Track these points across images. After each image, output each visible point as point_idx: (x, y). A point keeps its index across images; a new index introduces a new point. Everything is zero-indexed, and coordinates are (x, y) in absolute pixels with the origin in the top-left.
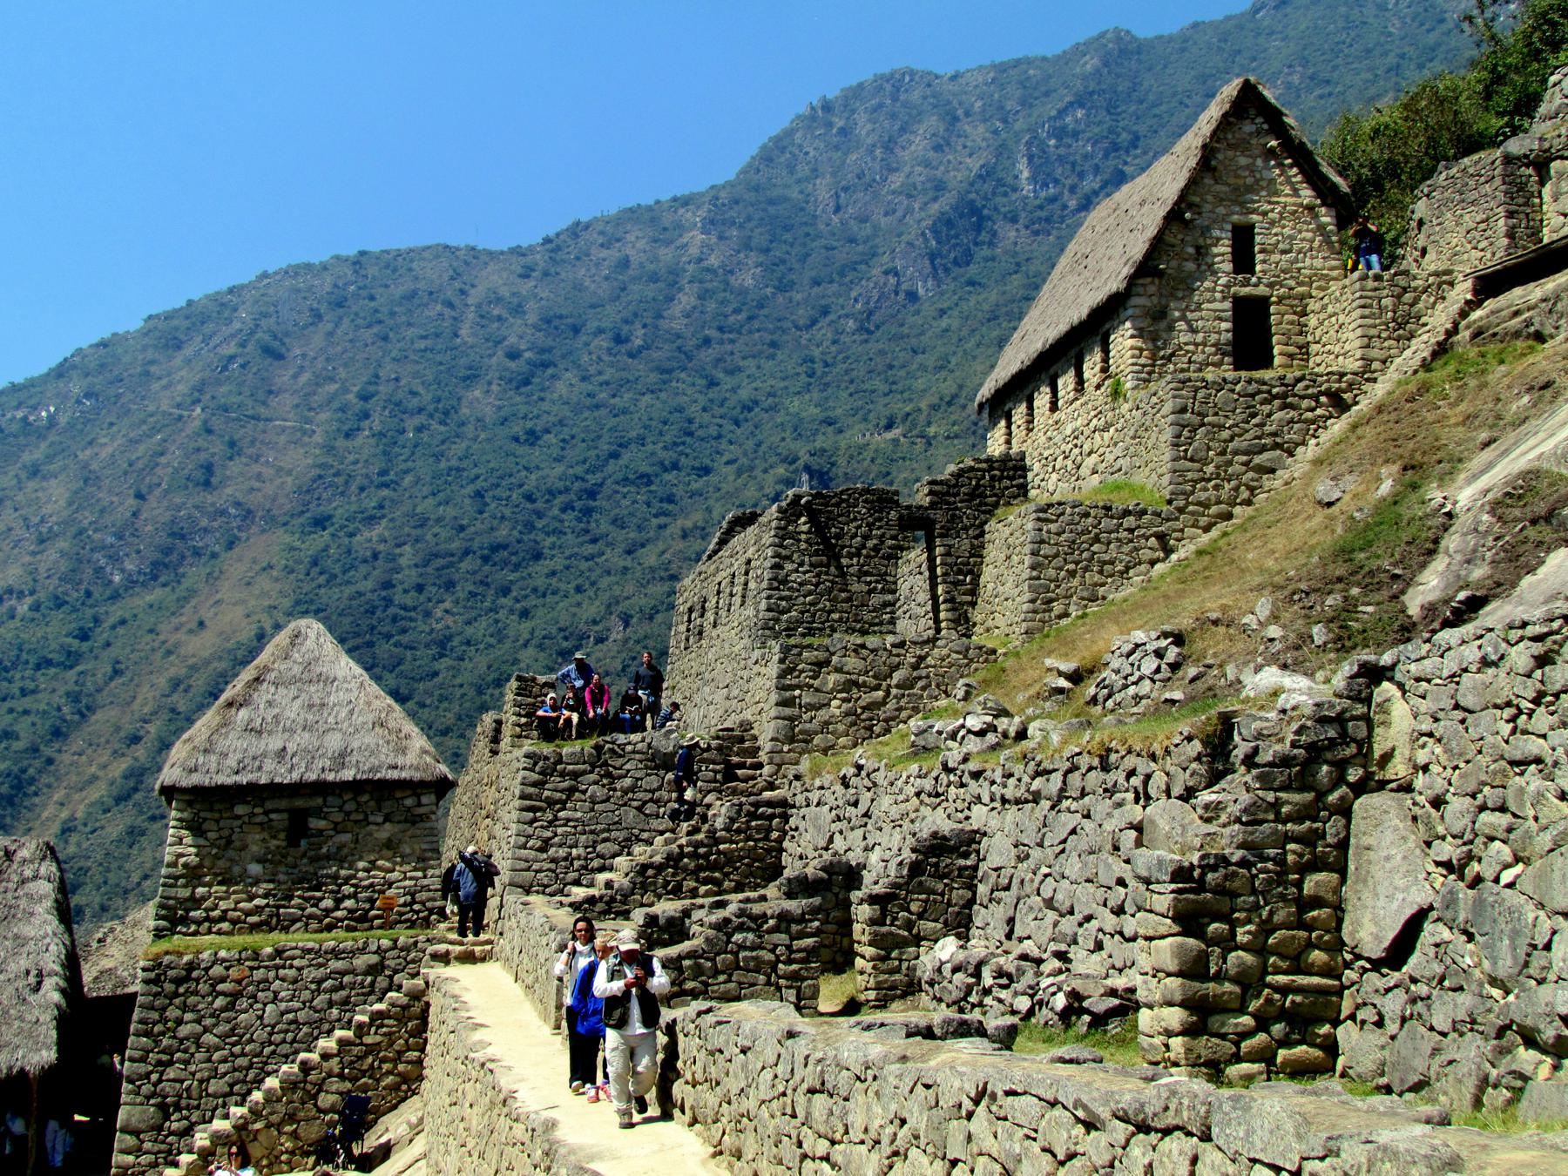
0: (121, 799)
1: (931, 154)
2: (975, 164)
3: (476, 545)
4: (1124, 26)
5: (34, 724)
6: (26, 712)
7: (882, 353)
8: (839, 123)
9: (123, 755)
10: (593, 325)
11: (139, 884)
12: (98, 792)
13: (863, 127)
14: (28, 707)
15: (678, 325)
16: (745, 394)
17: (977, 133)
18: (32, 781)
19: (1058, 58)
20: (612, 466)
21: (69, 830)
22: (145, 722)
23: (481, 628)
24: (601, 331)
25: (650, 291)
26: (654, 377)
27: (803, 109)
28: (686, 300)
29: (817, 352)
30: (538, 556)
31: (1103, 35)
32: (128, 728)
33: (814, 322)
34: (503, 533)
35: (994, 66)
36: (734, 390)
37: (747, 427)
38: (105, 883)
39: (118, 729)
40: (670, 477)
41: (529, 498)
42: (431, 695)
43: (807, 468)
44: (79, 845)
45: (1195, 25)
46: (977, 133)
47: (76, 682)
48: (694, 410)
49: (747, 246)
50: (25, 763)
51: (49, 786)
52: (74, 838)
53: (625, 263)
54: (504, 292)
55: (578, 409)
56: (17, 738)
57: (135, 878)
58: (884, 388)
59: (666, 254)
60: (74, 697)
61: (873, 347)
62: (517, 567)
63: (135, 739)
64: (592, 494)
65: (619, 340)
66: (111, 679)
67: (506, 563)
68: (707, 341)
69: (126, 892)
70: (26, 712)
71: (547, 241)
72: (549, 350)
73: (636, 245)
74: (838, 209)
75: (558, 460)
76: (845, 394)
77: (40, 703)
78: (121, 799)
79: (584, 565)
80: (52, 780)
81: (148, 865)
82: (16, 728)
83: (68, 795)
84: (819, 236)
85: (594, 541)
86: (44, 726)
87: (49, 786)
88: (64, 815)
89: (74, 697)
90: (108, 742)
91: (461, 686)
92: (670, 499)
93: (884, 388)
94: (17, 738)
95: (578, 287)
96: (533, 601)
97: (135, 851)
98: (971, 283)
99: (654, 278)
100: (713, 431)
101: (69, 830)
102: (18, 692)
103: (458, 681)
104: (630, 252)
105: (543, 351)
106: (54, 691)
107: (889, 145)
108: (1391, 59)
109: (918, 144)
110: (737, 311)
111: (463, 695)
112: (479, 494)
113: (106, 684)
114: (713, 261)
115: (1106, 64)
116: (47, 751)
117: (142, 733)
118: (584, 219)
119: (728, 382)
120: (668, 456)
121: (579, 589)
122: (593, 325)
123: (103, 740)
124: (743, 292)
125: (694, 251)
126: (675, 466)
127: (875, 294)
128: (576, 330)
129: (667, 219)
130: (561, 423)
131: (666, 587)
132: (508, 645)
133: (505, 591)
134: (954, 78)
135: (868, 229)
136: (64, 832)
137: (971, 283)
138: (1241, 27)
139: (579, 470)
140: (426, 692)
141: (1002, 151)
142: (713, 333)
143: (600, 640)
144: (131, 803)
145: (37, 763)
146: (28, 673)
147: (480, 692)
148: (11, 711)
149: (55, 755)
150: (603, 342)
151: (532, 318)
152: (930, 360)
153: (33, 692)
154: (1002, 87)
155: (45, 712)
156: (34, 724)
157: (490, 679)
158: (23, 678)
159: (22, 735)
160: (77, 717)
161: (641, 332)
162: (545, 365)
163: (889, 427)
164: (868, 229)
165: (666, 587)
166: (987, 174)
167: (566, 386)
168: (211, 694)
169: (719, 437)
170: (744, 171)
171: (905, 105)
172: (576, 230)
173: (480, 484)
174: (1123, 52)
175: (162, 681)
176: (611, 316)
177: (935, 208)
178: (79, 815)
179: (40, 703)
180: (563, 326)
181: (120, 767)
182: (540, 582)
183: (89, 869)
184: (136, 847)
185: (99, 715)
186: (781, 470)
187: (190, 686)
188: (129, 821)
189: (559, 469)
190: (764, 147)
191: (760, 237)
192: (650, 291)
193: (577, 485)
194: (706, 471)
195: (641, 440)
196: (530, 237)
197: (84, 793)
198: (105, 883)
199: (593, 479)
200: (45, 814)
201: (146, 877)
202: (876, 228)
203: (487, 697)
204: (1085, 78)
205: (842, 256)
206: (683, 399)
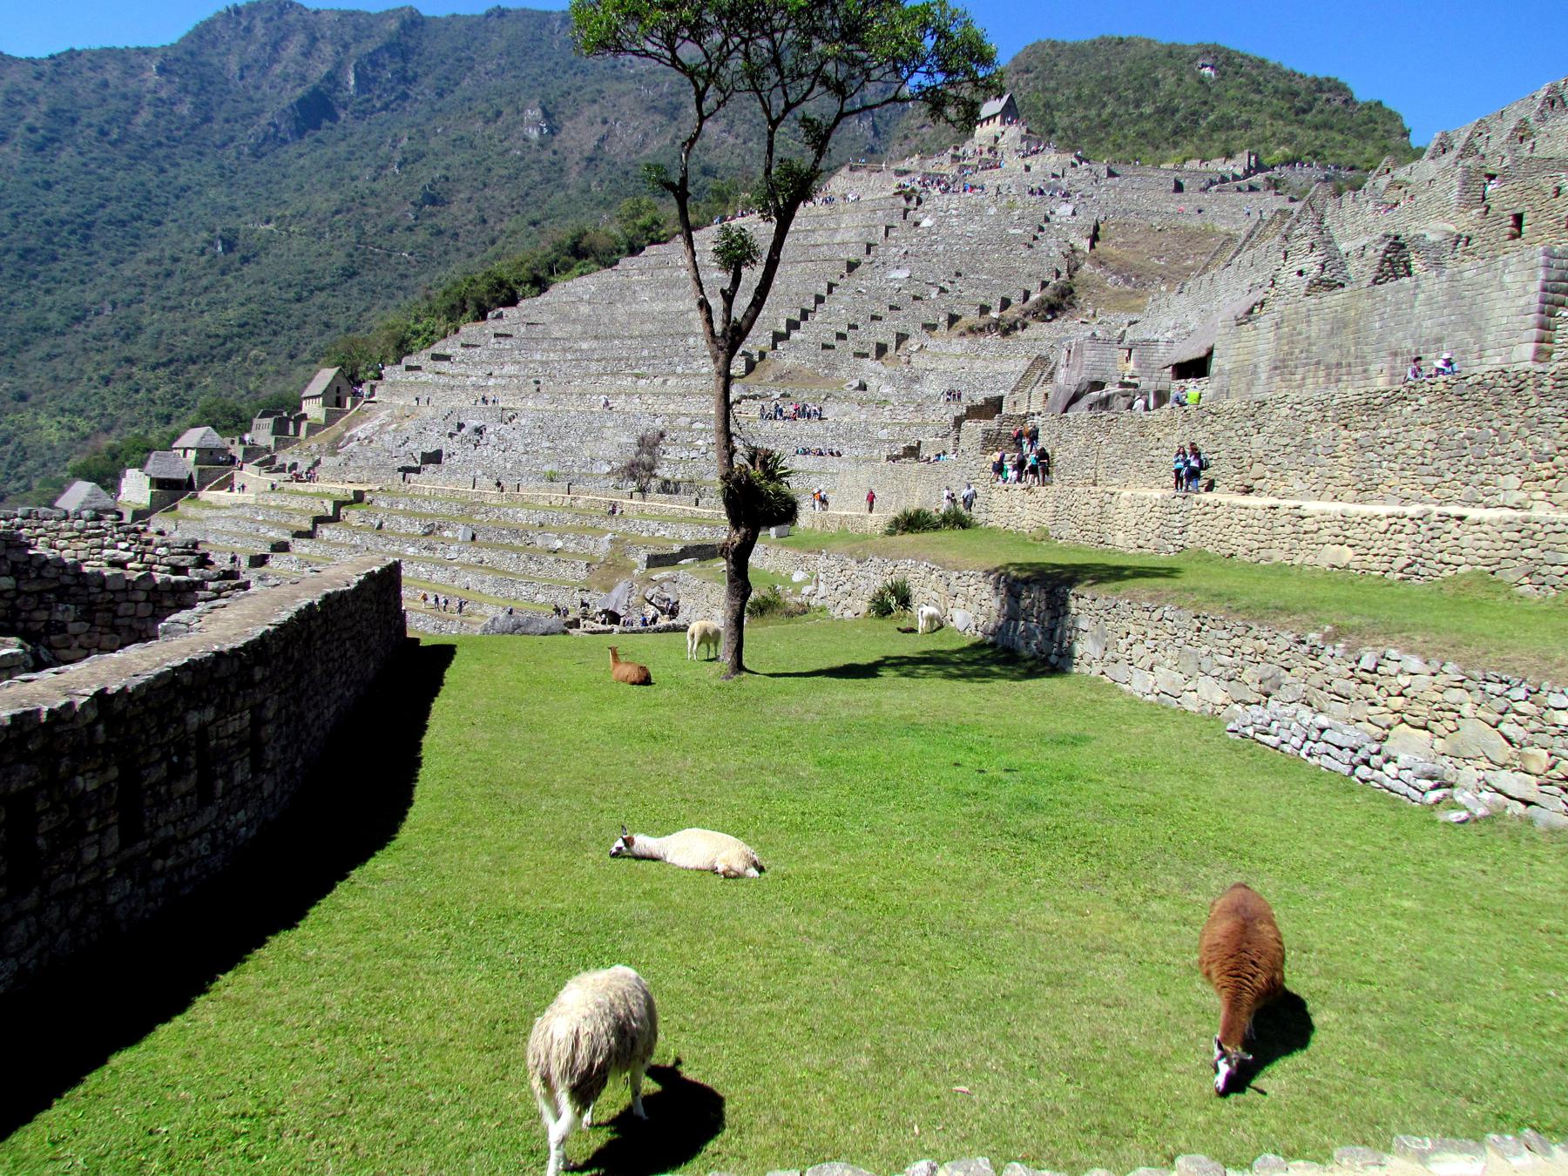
1: (300, 58)
2: (324, 69)
3: (14, 246)
4: (416, 5)
7: (265, 172)
8: (245, 23)
10: (85, 120)
13: (259, 30)
15: (139, 130)
16: (182, 181)
17: (327, 50)
19: (377, 15)
20: (100, 212)
23: (19, 296)
24: (90, 125)
25: (123, 105)
26: (125, 161)
27: (223, 9)
28: (145, 115)
29: (226, 163)
30: (55, 259)
31: (403, 9)
33: (224, 145)
34: (32, 242)
35: (339, 11)
36: (176, 177)
37: (182, 202)
40: (138, 224)
41: (48, 223)
43: (221, 237)
45: (454, 16)
46: (327, 50)
48: (150, 185)
49: (185, 89)
53: (105, 85)
54: (23, 87)
55: (77, 172)
58: (266, 194)
59: (133, 85)
61: (258, 167)
62: (41, 263)
64: (88, 226)
65: (103, 133)
67: (34, 260)
68: (160, 144)
71: (52, 57)
72: (57, 131)
73: (113, 74)
74: (242, 78)
75: (65, 202)
76: (242, 193)
79: (85, 268)
84: (230, 92)
85: (90, 254)
92: (137, 237)
93: (266, 194)
95: (74, 92)
96: (52, 285)
98: (318, 141)
99: (125, 97)
100: (163, 200)
104: (108, 76)
105: (52, 131)
107: (276, 47)
108: (550, 64)
109: (292, 49)
110: (178, 129)
112: (15, 216)
114: (163, 94)
115: (403, 26)
118: (78, 48)
119: (172, 172)
120: (136, 211)
121: (82, 282)
122: (85, 120)
124: (183, 118)
125: (151, 85)
126: (140, 218)
127: (262, 136)
128: (74, 121)
129: (134, 61)
130: (66, 179)
131: (138, 290)
132: (38, 308)
133: (35, 276)
134: (317, 12)
135: (258, 95)
137: (318, 141)
138: (479, 24)
139: (80, 211)
141: (339, 65)
142: (163, 140)
143: (97, 314)
147: (23, 332)
150: (93, 133)
151: (44, 108)
152: (292, 183)
154: (343, 26)
161: (116, 131)
162: (53, 140)
163: (268, 222)
164: (258, 95)
165: (138, 290)
166: (330, 77)
167: (66, 157)
169: (166, 204)
170: (182, 39)
171: (286, 23)
172: (72, 54)
173: (14, 209)
174: (414, 23)
176: (97, 116)
177: (300, 92)
180: (63, 118)
182: (58, 274)
186: (205, 235)
189: (66, 209)
190: (197, 27)
191: (193, 85)
192: (123, 105)
193: (79, 220)
194: (159, 223)
195: (119, 199)
196: (41, 53)
199: (89, 218)
202: (264, 95)
204: (391, 34)
205: (245, 107)
206: (142, 178)
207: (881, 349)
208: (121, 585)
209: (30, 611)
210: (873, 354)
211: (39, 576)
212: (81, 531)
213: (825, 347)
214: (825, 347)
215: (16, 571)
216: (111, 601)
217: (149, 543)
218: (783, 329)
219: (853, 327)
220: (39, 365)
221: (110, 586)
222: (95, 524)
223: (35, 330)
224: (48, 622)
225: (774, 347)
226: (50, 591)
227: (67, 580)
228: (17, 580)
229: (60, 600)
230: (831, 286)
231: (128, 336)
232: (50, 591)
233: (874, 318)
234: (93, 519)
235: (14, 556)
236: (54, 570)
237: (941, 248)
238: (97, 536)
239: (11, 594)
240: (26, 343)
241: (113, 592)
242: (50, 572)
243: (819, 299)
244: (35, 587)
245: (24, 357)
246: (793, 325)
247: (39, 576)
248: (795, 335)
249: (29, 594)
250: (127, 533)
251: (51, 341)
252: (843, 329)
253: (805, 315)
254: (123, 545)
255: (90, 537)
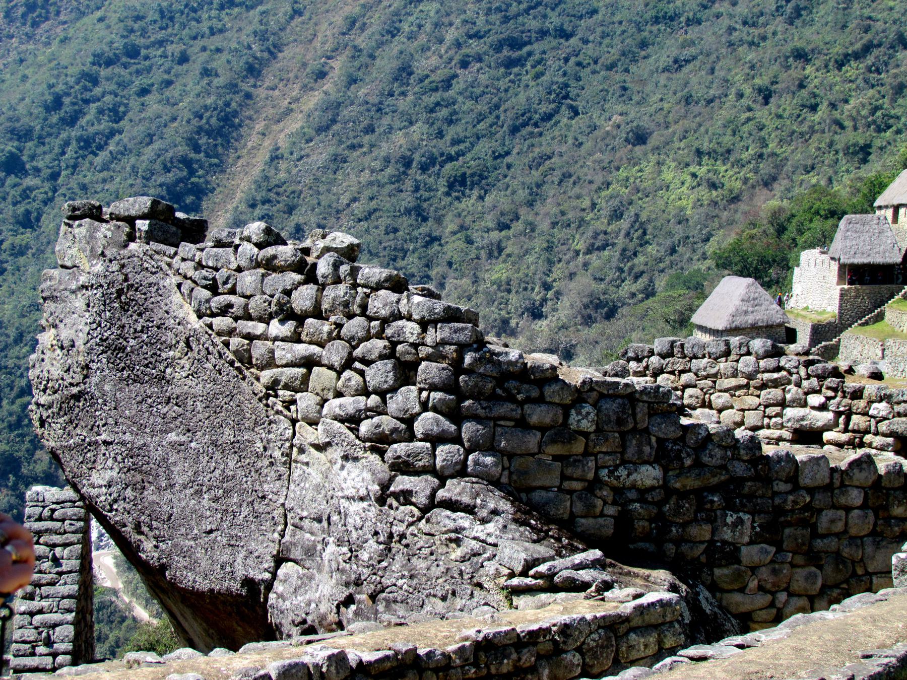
0: (322, 129)
5: (229, 62)
6: (218, 50)
9: (312, 89)
11: (348, 205)
12: (295, 124)
14: (219, 45)
18: (235, 114)
21: (277, 157)
22: (329, 58)
32: (314, 65)
38: (319, 204)
39: (304, 65)
42: (594, 32)
44: (288, 171)
47: (261, 22)
50: (228, 97)
51: (250, 118)
52: (283, 165)
56: (217, 75)
57: (344, 200)
60: (262, 36)
63: (321, 75)
66: (292, 18)
69: (338, 212)
70: (218, 50)
77: (231, 40)
78: (322, 129)
80: (252, 112)
81: (355, 189)
82: (214, 65)
83: (267, 127)
86: (240, 64)
87: (250, 118)
88: (267, 143)
89: (262, 36)
90: (296, 77)
91: (620, 23)
94: (217, 75)
97: (340, 176)
101: (277, 157)
102: (207, 32)
103: (617, 18)
106: (240, 30)
111: (624, 32)
113: (288, 22)
116: (245, 87)
117: (327, 69)
123: (291, 75)
136: (272, 159)
140: (588, 29)
144: (331, 132)
145: (237, 98)
146: (214, 13)
148: (204, 49)
149: (252, 90)
153: (221, 31)
155: (236, 50)
156: (229, 62)
157: (647, 16)
158: (210, 18)
159: (220, 71)
160: (266, 55)
168: (388, 32)
175: (338, 19)
178: (281, 143)
179: (231, 40)
181: (313, 100)
183: (301, 192)
184: (340, 172)
185: (288, 52)
187: (364, 24)
188: (331, 150)
197: (282, 124)
198: (319, 204)
200: (250, 144)
201: (355, 200)
203: (646, 34)
208: (822, 477)
209: (685, 525)
211: (698, 464)
212: (750, 377)
215: (664, 456)
216: (808, 507)
217: (857, 394)
220: (663, 79)
221: (806, 480)
222: (770, 363)
223: (656, 20)
224: (712, 542)
226: (713, 490)
227: (739, 469)
228: (666, 470)
229: (730, 506)
231: (798, 12)
232: (713, 490)
234: (768, 355)
235: (661, 429)
236: (718, 452)
238: (776, 384)
239: (657, 496)
240: (643, 45)
241: (811, 491)
242: (714, 457)
244: (691, 482)
245: (641, 69)
247: (698, 464)
249: (683, 494)
250: (821, 377)
251: (681, 37)
254: (815, 400)
255: (764, 386)
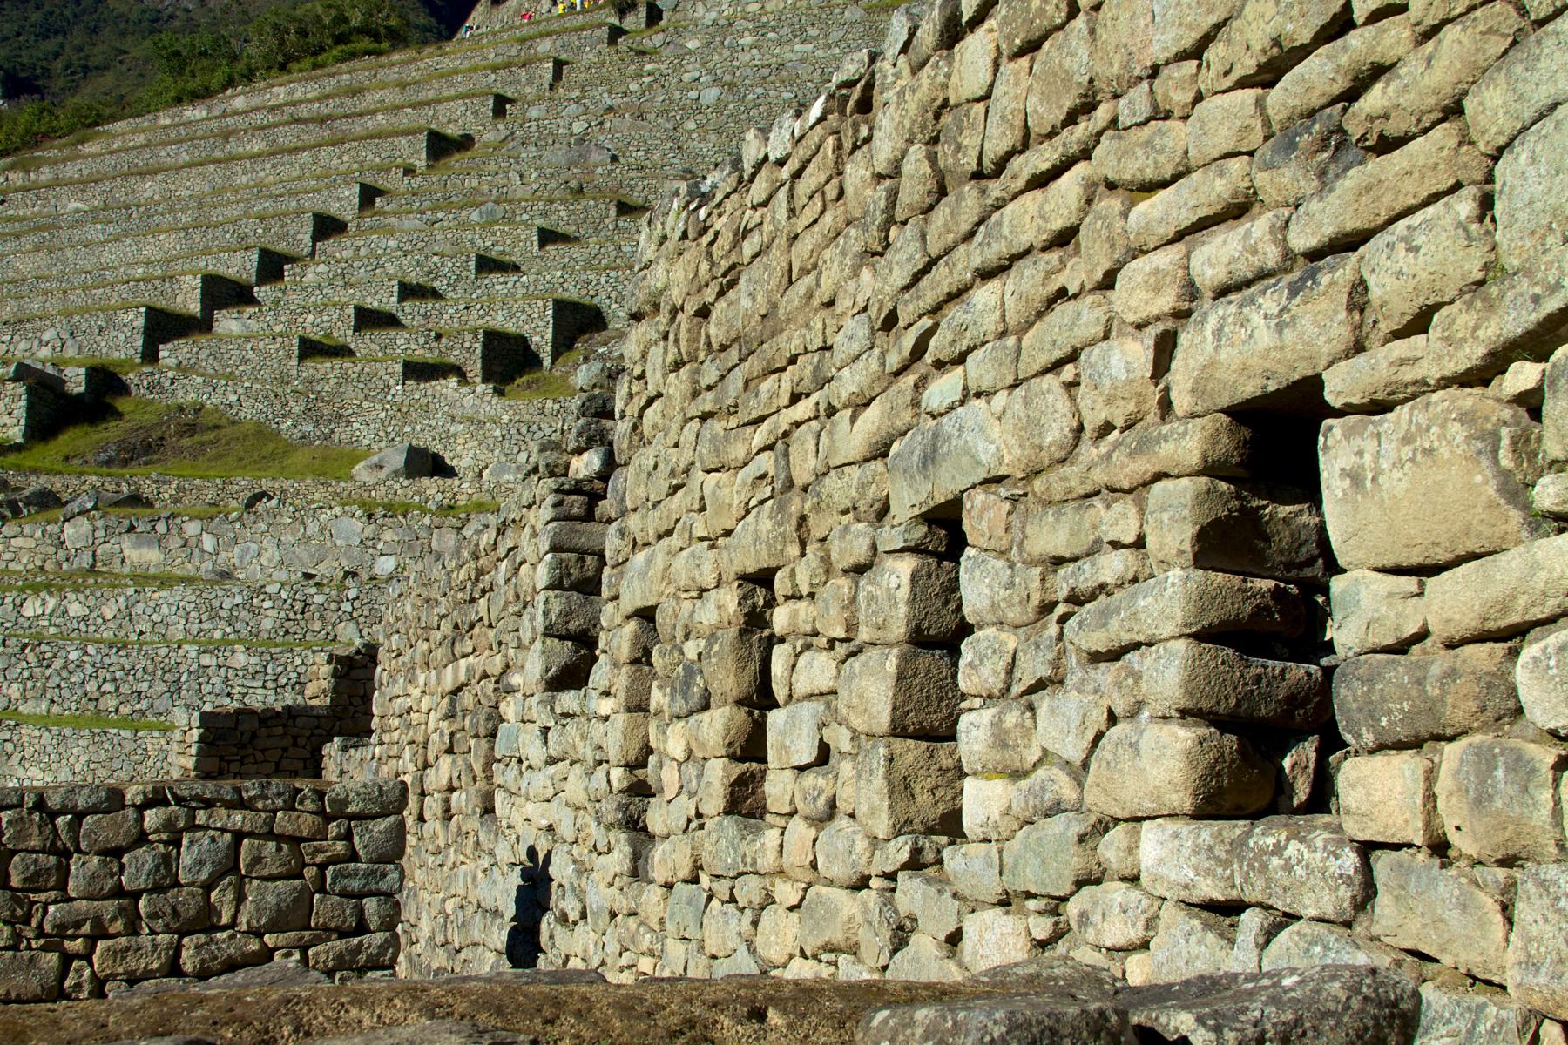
207: (507, 360)
210: (475, 367)
213: (310, 349)
214: (310, 349)
218: (194, 307)
219: (409, 291)
225: (150, 355)
230: (369, 195)
233: (487, 265)
237: (710, 95)
243: (327, 227)
246: (224, 293)
248: (228, 322)
252: (386, 300)
253: (272, 266)
